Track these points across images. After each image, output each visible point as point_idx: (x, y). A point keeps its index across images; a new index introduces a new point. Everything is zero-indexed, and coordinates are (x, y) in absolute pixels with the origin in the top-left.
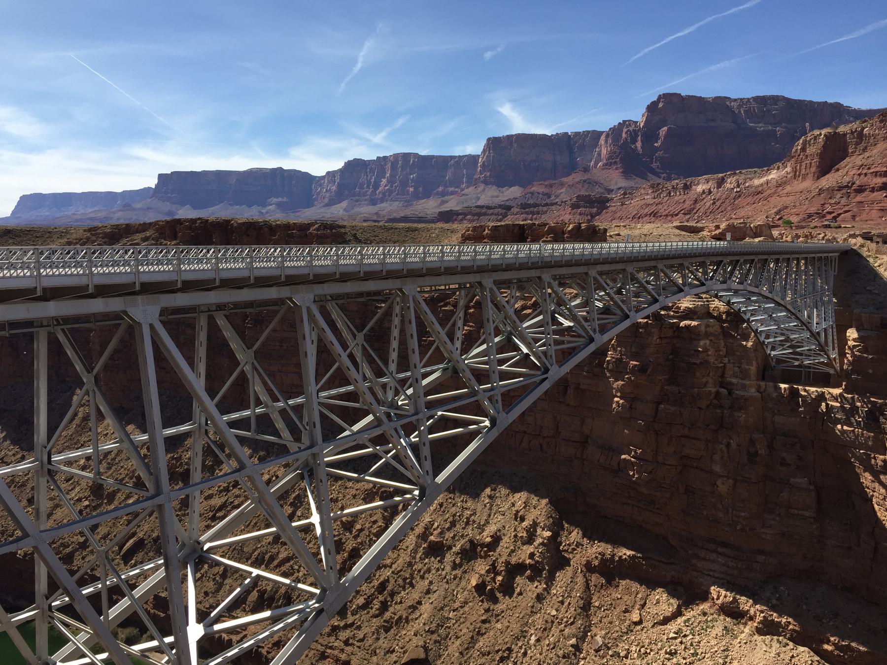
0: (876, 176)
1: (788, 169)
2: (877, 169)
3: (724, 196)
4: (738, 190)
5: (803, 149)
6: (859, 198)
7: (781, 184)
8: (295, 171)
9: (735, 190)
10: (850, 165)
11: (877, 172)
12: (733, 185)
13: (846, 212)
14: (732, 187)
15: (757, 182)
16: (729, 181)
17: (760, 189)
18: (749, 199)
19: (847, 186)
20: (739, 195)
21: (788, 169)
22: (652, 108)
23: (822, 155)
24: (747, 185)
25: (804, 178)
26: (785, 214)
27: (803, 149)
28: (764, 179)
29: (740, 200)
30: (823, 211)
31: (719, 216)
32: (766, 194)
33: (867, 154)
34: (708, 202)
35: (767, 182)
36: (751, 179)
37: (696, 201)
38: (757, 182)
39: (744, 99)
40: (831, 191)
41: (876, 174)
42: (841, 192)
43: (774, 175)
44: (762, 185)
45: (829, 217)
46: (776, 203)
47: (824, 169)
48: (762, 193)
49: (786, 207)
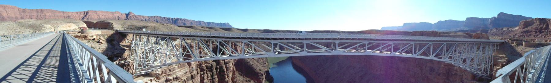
5: (521, 23)
7: (518, 30)
8: (426, 23)
15: (514, 29)
20: (511, 31)
22: (499, 15)
23: (524, 25)
25: (521, 28)
27: (521, 23)
34: (506, 32)
37: (503, 32)
38: (514, 29)
40: (525, 32)
43: (517, 28)
46: (515, 33)
47: (524, 28)
49: (517, 34)
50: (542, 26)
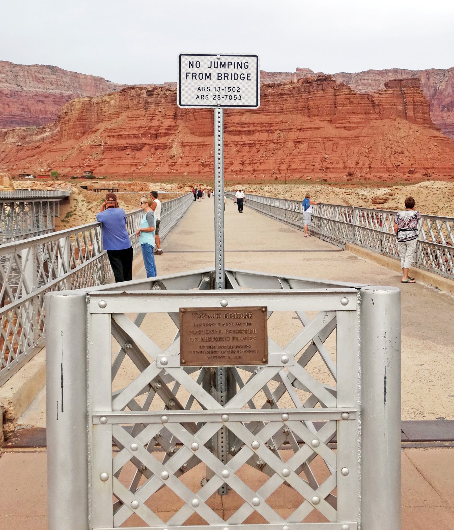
0: (121, 138)
1: (58, 129)
2: (122, 133)
3: (8, 149)
4: (20, 144)
6: (109, 155)
9: (17, 144)
10: (103, 128)
11: (121, 135)
12: (15, 139)
13: (101, 165)
14: (14, 141)
16: (11, 135)
17: (38, 144)
18: (29, 153)
19: (100, 145)
21: (58, 129)
24: (27, 140)
26: (54, 166)
28: (42, 136)
29: (21, 153)
30: (84, 164)
31: (4, 167)
32: (42, 148)
33: (114, 121)
35: (43, 139)
36: (31, 135)
39: (25, 65)
41: (120, 137)
42: (97, 149)
44: (39, 141)
45: (88, 169)
48: (39, 148)
50: (155, 123)
